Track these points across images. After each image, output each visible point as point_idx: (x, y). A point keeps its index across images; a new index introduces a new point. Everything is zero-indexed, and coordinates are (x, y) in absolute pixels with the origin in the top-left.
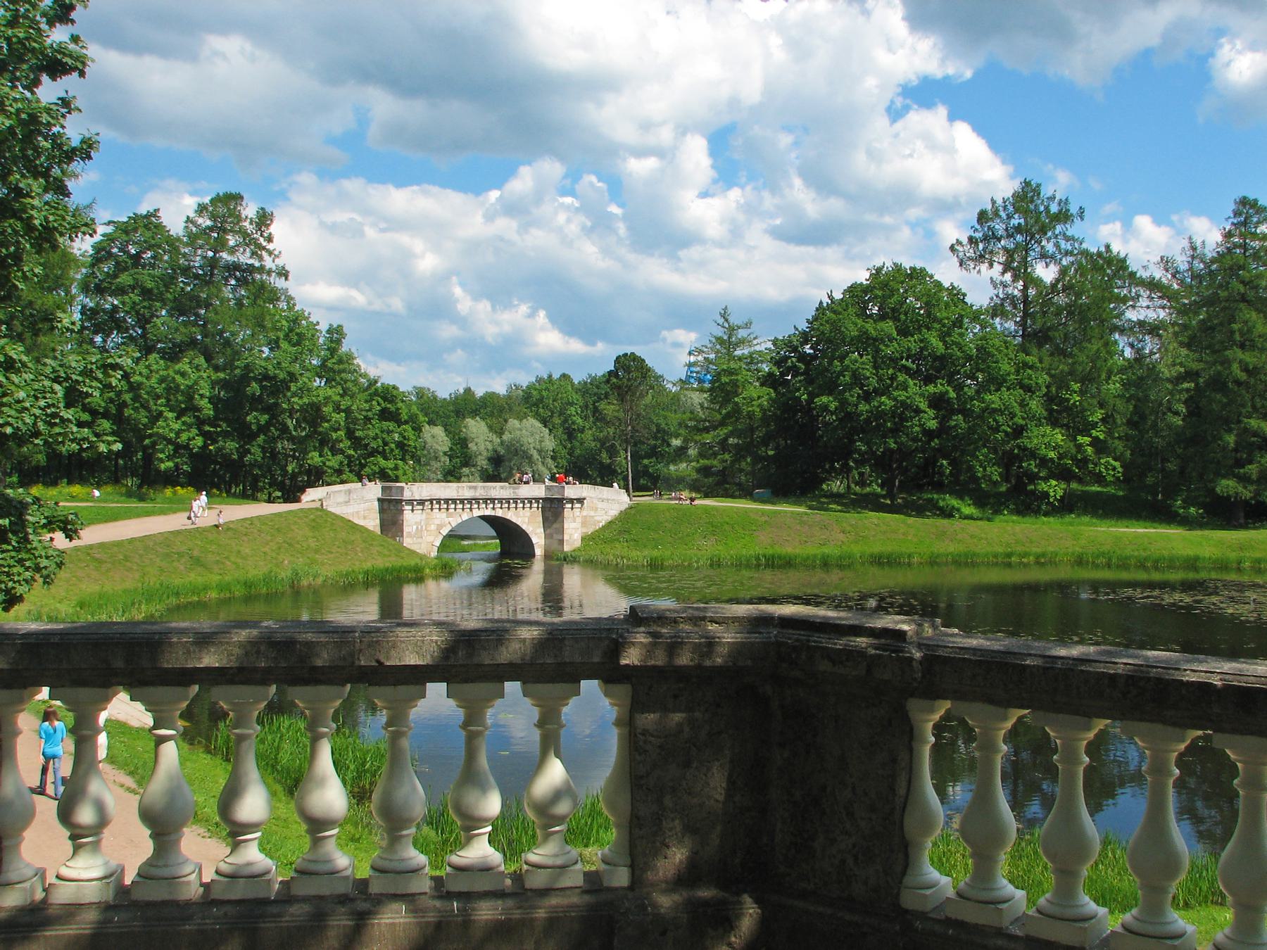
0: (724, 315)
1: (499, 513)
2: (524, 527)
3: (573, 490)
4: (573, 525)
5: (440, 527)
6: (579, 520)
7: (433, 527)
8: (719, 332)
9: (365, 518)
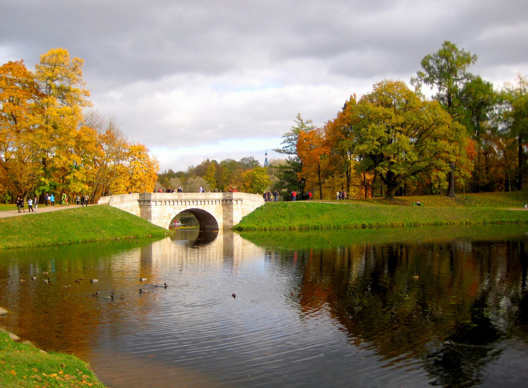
0: (299, 118)
1: (200, 207)
2: (212, 214)
3: (236, 195)
5: (170, 215)
6: (240, 210)
7: (166, 215)
8: (296, 126)
9: (131, 210)
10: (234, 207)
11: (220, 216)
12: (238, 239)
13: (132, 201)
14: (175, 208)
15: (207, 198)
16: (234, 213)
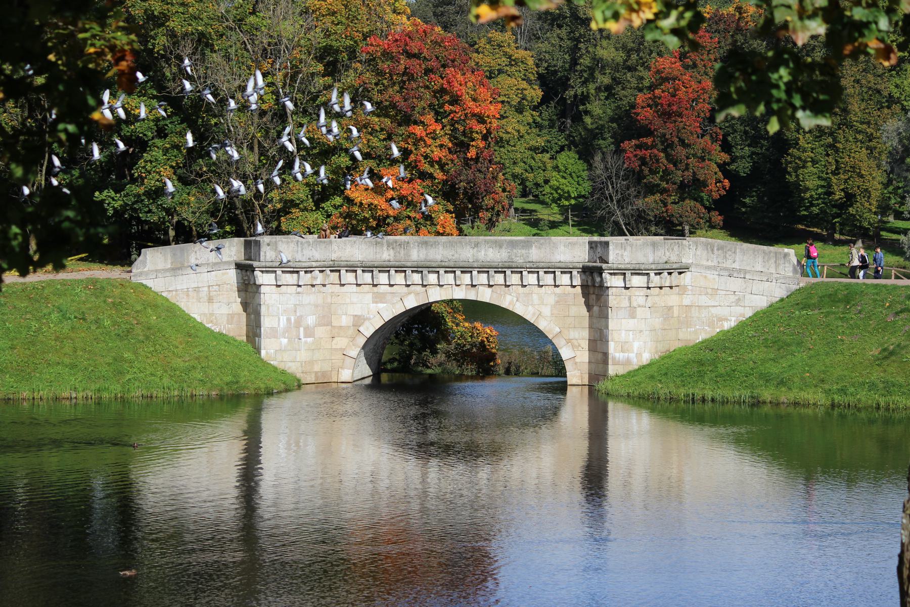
1: (485, 295)
2: (542, 325)
3: (624, 250)
4: (631, 323)
5: (358, 321)
7: (345, 321)
9: (210, 300)
10: (612, 300)
11: (574, 334)
12: (634, 437)
13: (214, 267)
14: (379, 298)
15: (520, 261)
16: (612, 324)
